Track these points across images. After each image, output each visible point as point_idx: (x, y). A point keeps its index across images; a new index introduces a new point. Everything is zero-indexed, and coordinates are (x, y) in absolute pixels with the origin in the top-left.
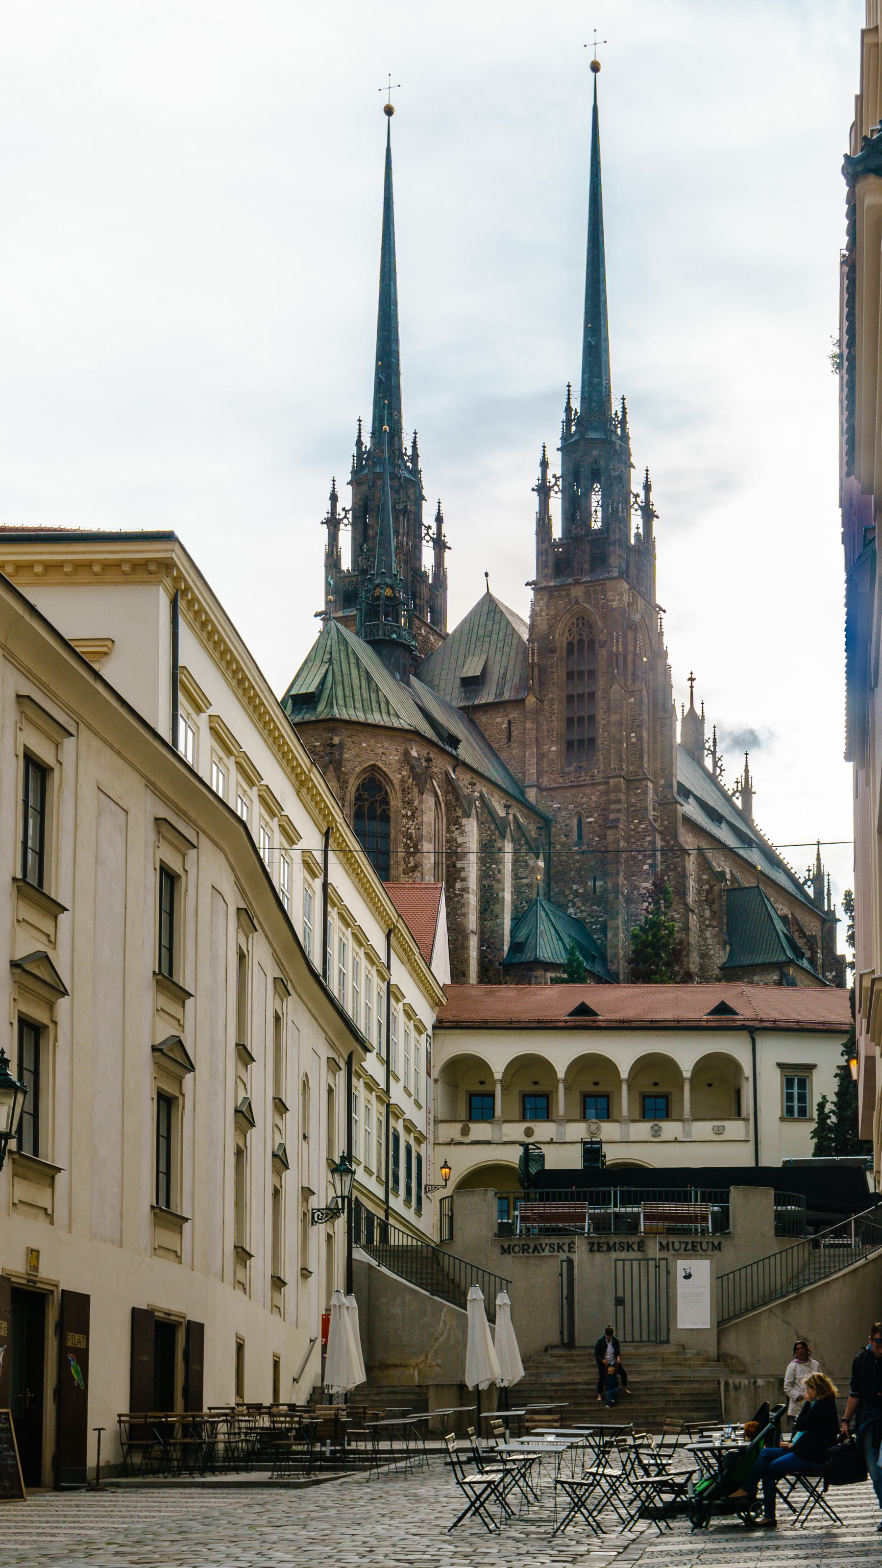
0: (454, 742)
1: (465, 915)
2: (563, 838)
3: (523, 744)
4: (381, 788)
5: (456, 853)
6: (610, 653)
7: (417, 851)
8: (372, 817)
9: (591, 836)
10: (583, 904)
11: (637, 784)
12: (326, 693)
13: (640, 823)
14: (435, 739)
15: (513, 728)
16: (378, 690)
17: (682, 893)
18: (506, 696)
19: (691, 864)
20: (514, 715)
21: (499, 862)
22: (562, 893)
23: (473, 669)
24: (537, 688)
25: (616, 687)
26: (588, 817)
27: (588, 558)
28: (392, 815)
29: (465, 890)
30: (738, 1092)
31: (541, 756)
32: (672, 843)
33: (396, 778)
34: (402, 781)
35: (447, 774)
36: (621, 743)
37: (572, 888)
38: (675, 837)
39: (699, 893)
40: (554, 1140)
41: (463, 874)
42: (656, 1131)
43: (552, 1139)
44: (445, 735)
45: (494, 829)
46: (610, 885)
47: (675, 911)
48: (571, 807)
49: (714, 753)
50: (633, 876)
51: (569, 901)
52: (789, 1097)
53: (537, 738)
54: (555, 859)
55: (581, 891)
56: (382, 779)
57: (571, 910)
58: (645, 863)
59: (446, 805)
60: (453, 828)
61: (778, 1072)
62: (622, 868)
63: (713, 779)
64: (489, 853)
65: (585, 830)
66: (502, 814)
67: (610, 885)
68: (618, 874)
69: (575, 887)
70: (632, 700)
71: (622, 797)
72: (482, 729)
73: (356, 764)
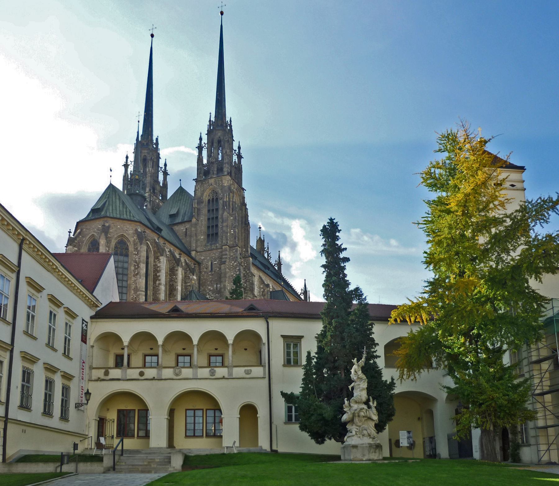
0: (160, 230)
1: (160, 294)
2: (205, 270)
3: (191, 236)
4: (125, 243)
5: (157, 270)
6: (223, 202)
7: (139, 267)
8: (121, 255)
11: (233, 248)
12: (105, 208)
14: (152, 228)
16: (126, 208)
17: (252, 290)
18: (185, 220)
19: (256, 280)
20: (188, 226)
21: (176, 275)
22: (204, 290)
23: (174, 211)
24: (196, 216)
25: (225, 213)
27: (216, 169)
28: (130, 254)
29: (160, 284)
30: (260, 352)
31: (197, 241)
33: (131, 240)
34: (134, 241)
35: (155, 240)
36: (227, 233)
38: (249, 269)
39: (260, 292)
40: (156, 378)
41: (159, 278)
42: (212, 373)
43: (154, 378)
44: (156, 227)
45: (174, 263)
46: (222, 286)
48: (208, 258)
49: (268, 252)
52: (288, 354)
53: (196, 234)
55: (212, 289)
59: (154, 252)
60: (156, 260)
61: (282, 340)
62: (227, 279)
63: (268, 260)
64: (172, 272)
65: (214, 266)
66: (178, 256)
67: (222, 286)
68: (225, 281)
71: (227, 253)
72: (176, 232)
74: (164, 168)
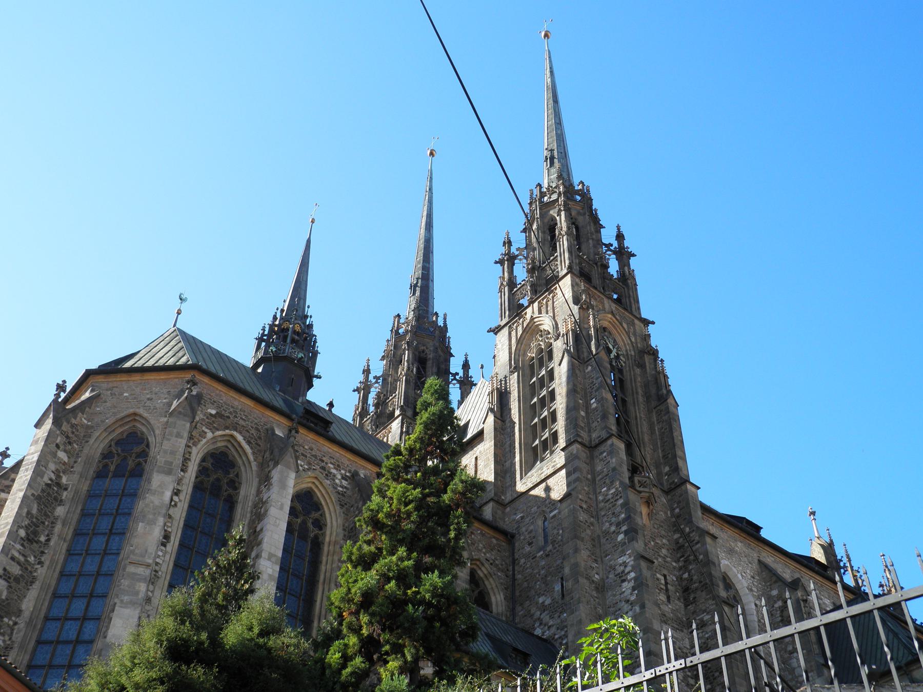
2: (528, 549)
9: (555, 532)
10: (551, 618)
11: (602, 448)
13: (609, 489)
15: (479, 462)
26: (551, 512)
29: (258, 556)
32: (687, 530)
37: (537, 603)
47: (704, 611)
48: (534, 509)
50: (606, 556)
51: (535, 622)
54: (520, 576)
56: (144, 430)
57: (538, 632)
58: (619, 533)
69: (541, 600)
70: (590, 368)
73: (108, 416)
74: (461, 374)
